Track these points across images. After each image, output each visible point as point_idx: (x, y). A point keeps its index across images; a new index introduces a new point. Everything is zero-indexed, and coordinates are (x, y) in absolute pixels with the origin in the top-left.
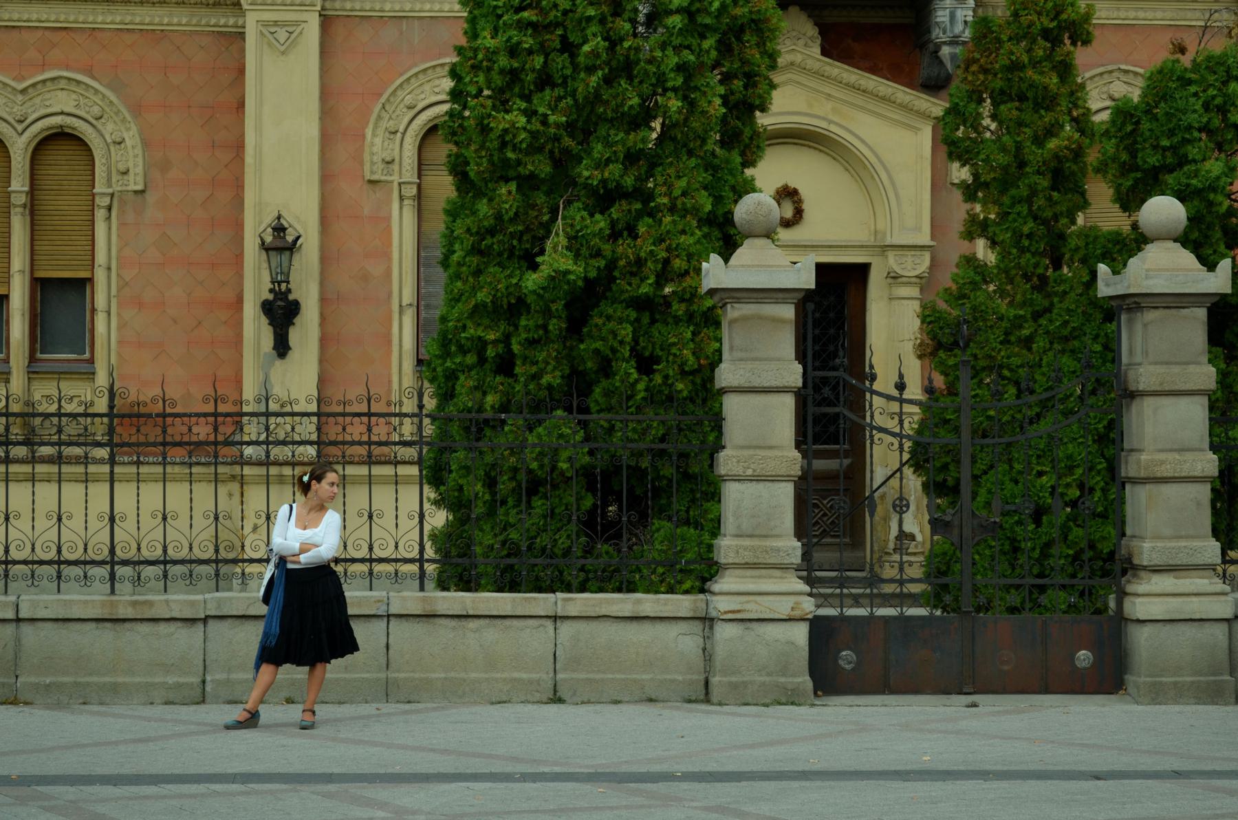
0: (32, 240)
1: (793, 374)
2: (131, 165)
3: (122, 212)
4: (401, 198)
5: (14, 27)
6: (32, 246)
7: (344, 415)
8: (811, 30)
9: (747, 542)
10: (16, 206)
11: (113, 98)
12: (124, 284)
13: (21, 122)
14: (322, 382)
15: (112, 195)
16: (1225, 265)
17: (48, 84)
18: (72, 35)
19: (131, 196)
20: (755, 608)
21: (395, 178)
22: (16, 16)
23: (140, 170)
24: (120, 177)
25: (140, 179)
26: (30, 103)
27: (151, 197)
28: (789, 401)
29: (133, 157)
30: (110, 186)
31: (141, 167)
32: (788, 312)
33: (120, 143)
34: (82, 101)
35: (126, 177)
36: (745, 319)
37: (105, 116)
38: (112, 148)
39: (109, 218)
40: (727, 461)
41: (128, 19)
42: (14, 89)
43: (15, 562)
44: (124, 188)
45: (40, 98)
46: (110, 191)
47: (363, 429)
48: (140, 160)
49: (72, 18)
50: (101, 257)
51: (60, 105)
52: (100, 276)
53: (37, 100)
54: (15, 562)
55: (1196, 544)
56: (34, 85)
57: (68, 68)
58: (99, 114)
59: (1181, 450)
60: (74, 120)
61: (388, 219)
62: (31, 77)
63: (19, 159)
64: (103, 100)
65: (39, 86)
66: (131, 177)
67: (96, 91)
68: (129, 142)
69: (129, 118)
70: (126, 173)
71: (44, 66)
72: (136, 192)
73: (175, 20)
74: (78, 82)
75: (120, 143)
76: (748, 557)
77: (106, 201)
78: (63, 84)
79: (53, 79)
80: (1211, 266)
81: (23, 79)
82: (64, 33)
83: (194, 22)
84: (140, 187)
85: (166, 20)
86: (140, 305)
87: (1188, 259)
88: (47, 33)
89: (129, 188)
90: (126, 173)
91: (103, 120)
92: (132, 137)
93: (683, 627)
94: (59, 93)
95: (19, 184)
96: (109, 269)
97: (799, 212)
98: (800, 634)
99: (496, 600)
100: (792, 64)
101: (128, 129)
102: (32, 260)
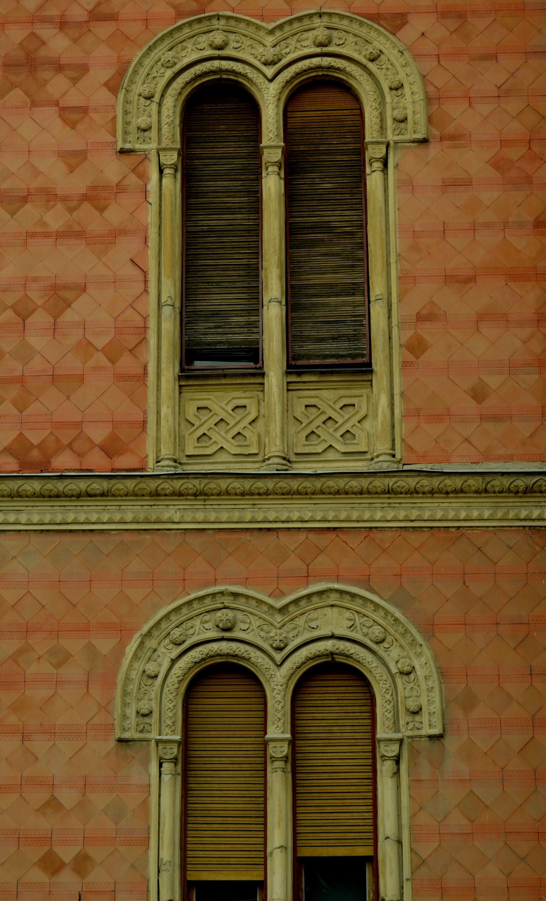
0: (295, 807)
2: (423, 701)
3: (414, 764)
5: (269, 529)
6: (294, 814)
10: (274, 759)
11: (398, 614)
12: (419, 864)
13: (279, 649)
15: (401, 741)
17: (315, 599)
18: (341, 536)
19: (425, 742)
22: (272, 516)
23: (436, 707)
24: (410, 718)
25: (437, 720)
26: (290, 626)
27: (451, 744)
29: (427, 693)
30: (398, 730)
31: (437, 704)
33: (408, 674)
34: (358, 620)
35: (417, 718)
37: (389, 639)
38: (399, 681)
39: (397, 773)
41: (414, 514)
42: (271, 607)
44: (416, 733)
45: (304, 618)
46: (399, 736)
48: (436, 696)
49: (343, 516)
50: (387, 825)
51: (330, 625)
52: (387, 853)
53: (301, 621)
56: (296, 602)
57: (338, 579)
58: (381, 636)
60: (348, 644)
62: (290, 593)
63: (279, 697)
64: (385, 618)
65: (303, 603)
66: (425, 717)
67: (377, 606)
68: (420, 672)
69: (419, 638)
70: (417, 712)
71: (307, 577)
72: (431, 737)
73: (475, 514)
74: (353, 596)
75: (408, 674)
77: (394, 749)
78: (333, 598)
79: (320, 593)
81: (283, 594)
82: (332, 536)
83: (499, 515)
84: (436, 731)
85: (463, 515)
88: (312, 536)
89: (423, 732)
90: (417, 712)
91: (385, 645)
92: (424, 664)
94: (328, 611)
95: (278, 730)
96: (399, 842)
101: (419, 655)
102: (295, 834)
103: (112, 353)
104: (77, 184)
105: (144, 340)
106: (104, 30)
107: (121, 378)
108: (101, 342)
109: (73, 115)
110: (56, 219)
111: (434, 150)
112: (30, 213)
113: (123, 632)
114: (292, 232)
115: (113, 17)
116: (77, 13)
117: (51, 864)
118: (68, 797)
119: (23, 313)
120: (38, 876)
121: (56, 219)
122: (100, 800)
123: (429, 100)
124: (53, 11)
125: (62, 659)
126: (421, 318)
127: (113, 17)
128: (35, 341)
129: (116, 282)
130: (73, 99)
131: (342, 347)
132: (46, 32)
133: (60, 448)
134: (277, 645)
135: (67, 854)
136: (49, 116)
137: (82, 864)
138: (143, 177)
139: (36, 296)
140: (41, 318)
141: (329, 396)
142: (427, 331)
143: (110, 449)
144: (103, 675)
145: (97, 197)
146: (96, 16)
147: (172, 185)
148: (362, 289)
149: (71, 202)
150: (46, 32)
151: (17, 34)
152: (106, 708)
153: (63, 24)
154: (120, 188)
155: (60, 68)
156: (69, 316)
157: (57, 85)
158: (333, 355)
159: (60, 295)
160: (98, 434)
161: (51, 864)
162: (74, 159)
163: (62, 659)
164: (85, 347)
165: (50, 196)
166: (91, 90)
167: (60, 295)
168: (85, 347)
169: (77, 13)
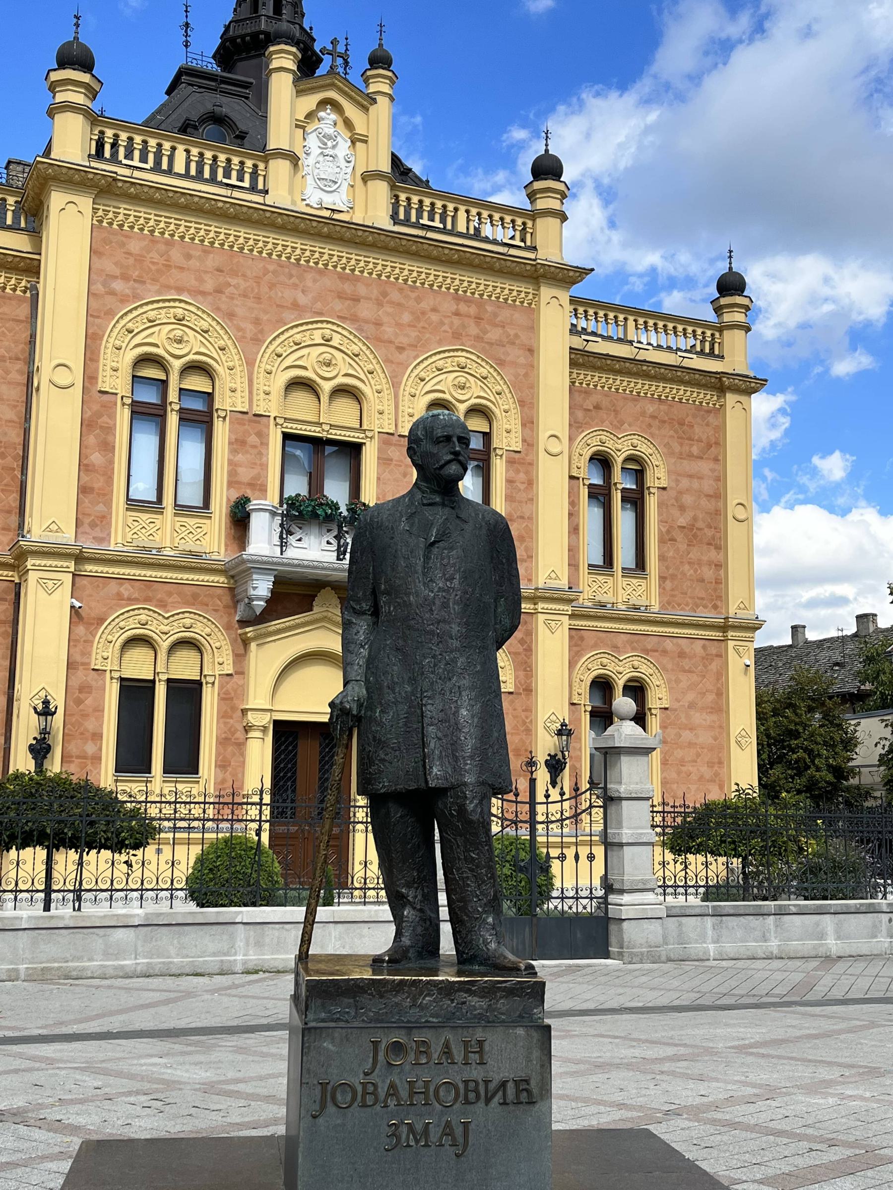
4: (112, 678)
7: (161, 802)
21: (108, 668)
43: (21, 891)
47: (201, 811)
54: (21, 891)
99: (285, 912)
100: (326, 617)
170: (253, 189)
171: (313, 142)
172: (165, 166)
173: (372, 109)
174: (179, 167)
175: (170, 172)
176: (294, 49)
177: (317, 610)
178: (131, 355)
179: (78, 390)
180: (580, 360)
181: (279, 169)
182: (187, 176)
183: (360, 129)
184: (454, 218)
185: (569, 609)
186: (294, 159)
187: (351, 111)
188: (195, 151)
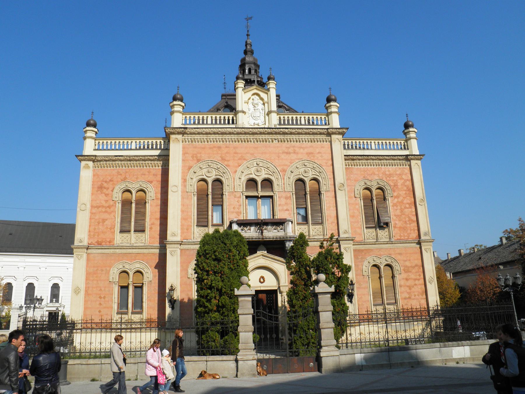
1: (252, 311)
8: (265, 249)
9: (244, 345)
14: (181, 314)
16: (333, 286)
20: (245, 358)
28: (251, 316)
32: (250, 299)
36: (242, 301)
40: (240, 329)
51: (137, 266)
55: (331, 341)
59: (327, 322)
61: (192, 284)
71: (135, 260)
76: (244, 347)
80: (331, 287)
86: (151, 301)
87: (326, 285)
93: (232, 362)
97: (264, 281)
98: (255, 362)
103: (111, 229)
104: (107, 205)
105: (115, 227)
106: (111, 183)
107: (112, 232)
108: (109, 227)
109: (107, 195)
110: (104, 210)
111: (155, 201)
112: (100, 209)
113: (110, 267)
114: (136, 212)
115: (113, 181)
116: (108, 180)
117: (100, 298)
118: (103, 289)
119: (99, 223)
120: (99, 299)
121: (104, 210)
122: (107, 289)
123: (155, 194)
124: (105, 180)
125: (102, 270)
126: (152, 224)
127: (113, 181)
128: (100, 227)
129: (111, 219)
130: (107, 193)
131: (141, 228)
132: (103, 183)
133: (103, 242)
134: (131, 268)
135: (102, 296)
136: (104, 194)
137: (104, 297)
138: (116, 204)
139: (101, 221)
140: (101, 224)
141: (139, 234)
142: (153, 226)
143: (110, 242)
144: (108, 272)
145: (109, 207)
146: (111, 181)
147: (120, 205)
148: (144, 220)
149: (106, 207)
150: (103, 183)
151: (100, 183)
152: (108, 277)
153: (106, 182)
154: (113, 205)
155: (105, 188)
156: (105, 223)
157: (105, 191)
158: (140, 230)
159: (104, 220)
160: (108, 240)
161: (100, 298)
162: (106, 201)
163: (102, 270)
164: (107, 228)
165: (103, 207)
166: (109, 191)
167: (104, 220)
168: (107, 228)
169: (108, 180)
170: (233, 123)
171: (251, 106)
172: (205, 123)
173: (269, 93)
174: (209, 122)
175: (207, 124)
176: (242, 81)
177: (259, 253)
178: (195, 180)
179: (180, 192)
180: (348, 158)
181: (240, 115)
182: (212, 123)
183: (266, 99)
184: (300, 120)
185: (352, 242)
186: (244, 112)
187: (263, 95)
188: (214, 116)
